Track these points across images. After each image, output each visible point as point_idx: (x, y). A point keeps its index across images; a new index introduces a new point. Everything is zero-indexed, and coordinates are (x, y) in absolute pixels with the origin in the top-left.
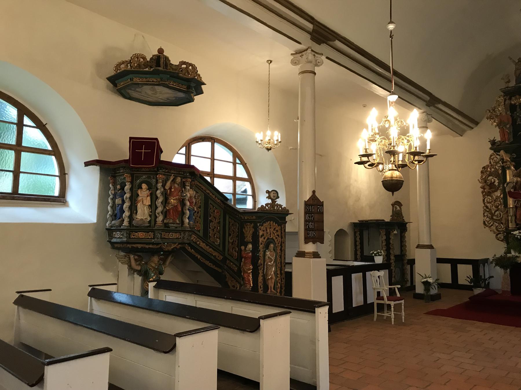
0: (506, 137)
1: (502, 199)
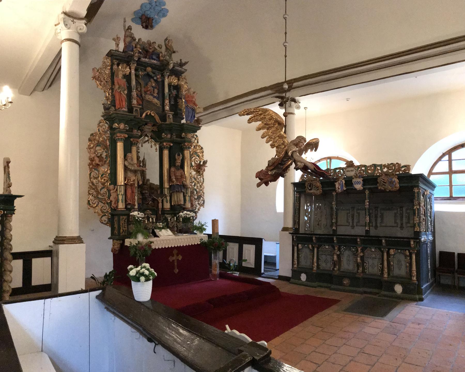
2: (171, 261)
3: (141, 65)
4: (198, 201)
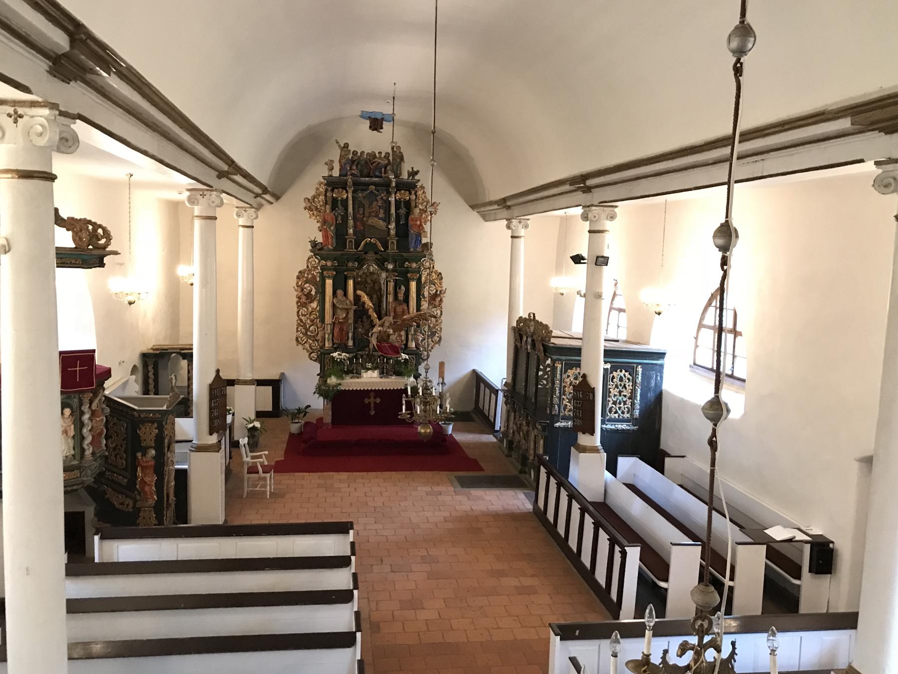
0: (330, 240)
1: (318, 312)
2: (367, 402)
3: (358, 186)
4: (432, 338)
